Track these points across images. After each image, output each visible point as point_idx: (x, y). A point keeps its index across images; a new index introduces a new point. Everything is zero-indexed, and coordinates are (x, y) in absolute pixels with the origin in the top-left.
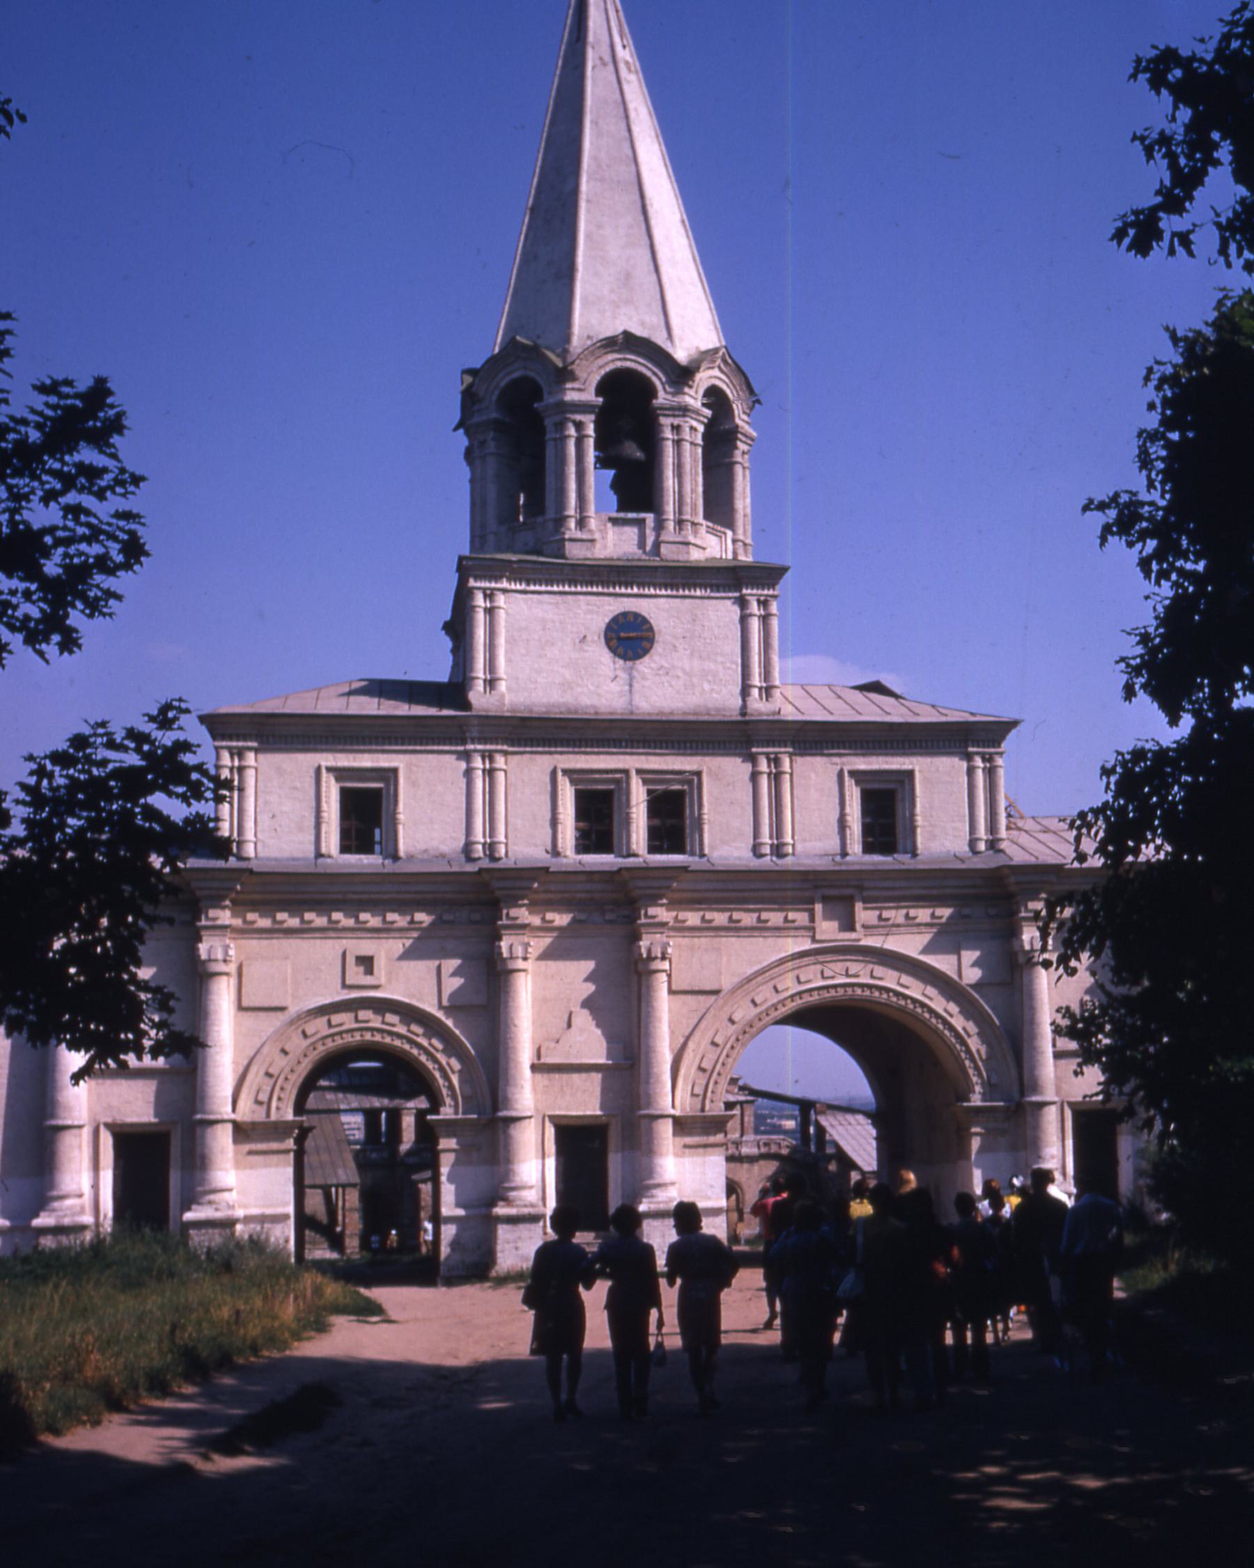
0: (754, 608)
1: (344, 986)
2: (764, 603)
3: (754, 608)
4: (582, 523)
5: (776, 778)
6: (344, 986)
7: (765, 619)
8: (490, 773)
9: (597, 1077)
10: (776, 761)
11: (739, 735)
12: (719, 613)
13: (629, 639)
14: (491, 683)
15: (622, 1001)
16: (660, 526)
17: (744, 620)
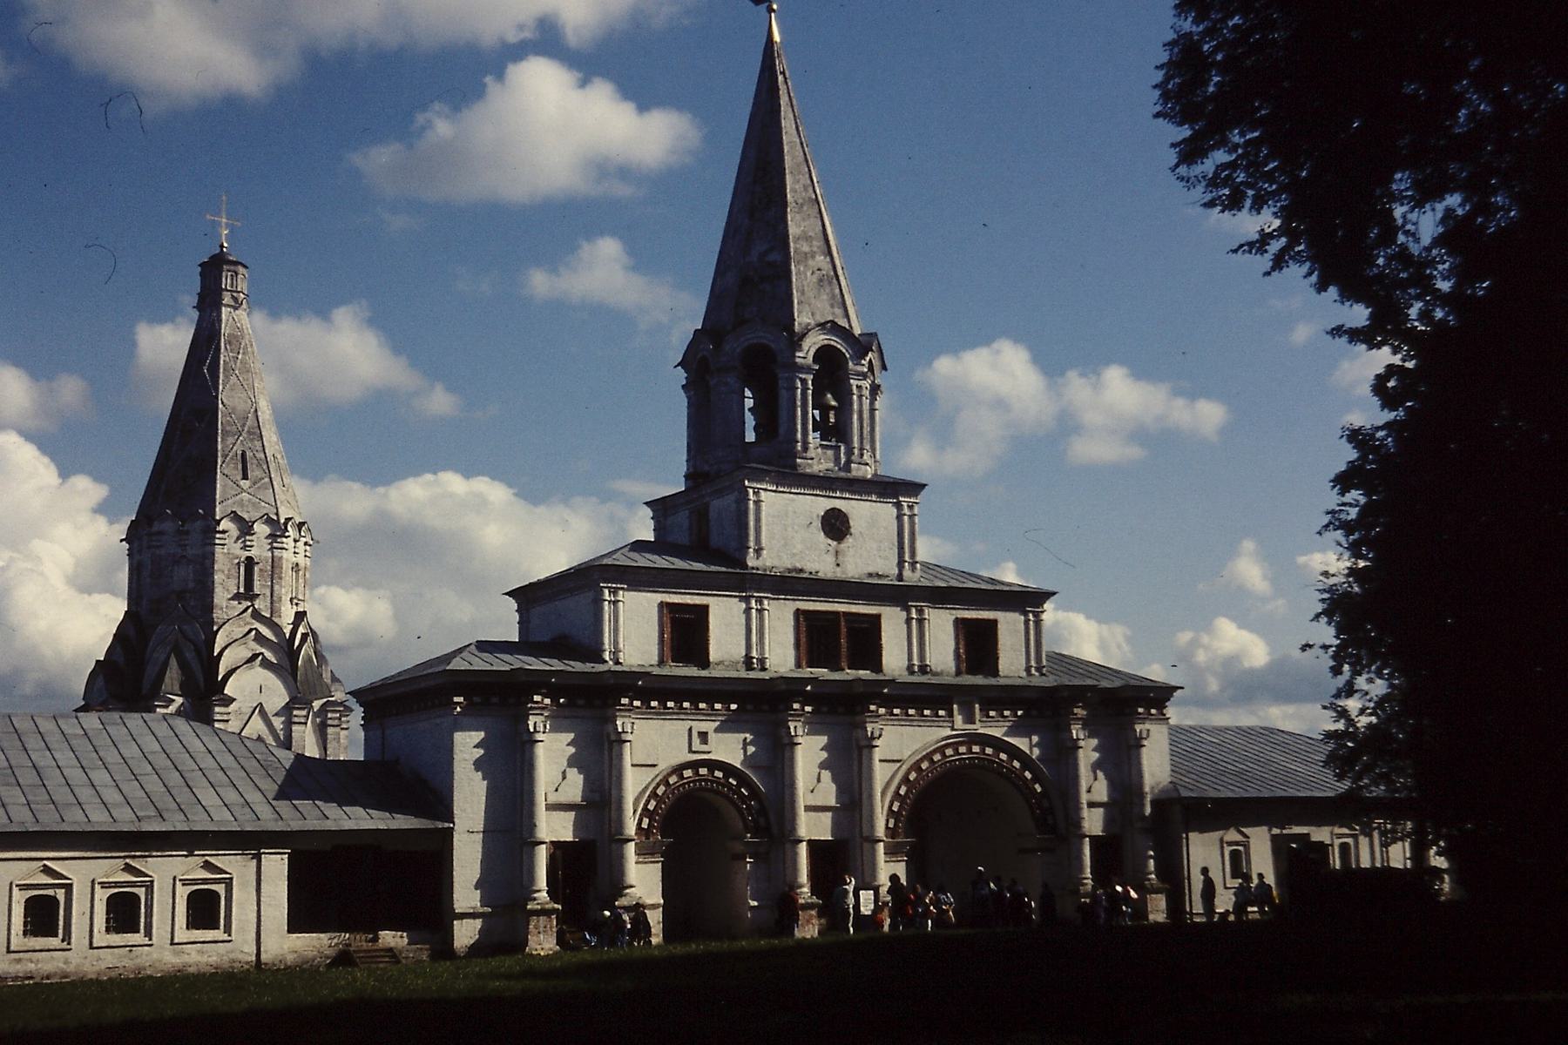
0: (906, 511)
1: (691, 751)
2: (911, 507)
3: (906, 511)
4: (805, 449)
5: (921, 621)
6: (691, 751)
7: (912, 517)
8: (760, 611)
9: (829, 814)
10: (920, 611)
11: (899, 595)
12: (886, 511)
13: (835, 525)
14: (758, 551)
15: (849, 763)
16: (849, 452)
17: (899, 517)
